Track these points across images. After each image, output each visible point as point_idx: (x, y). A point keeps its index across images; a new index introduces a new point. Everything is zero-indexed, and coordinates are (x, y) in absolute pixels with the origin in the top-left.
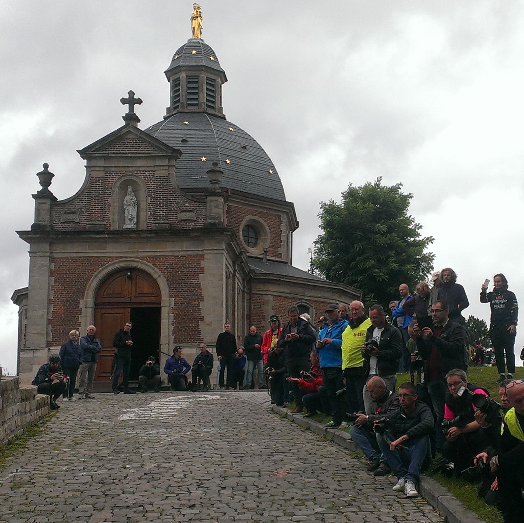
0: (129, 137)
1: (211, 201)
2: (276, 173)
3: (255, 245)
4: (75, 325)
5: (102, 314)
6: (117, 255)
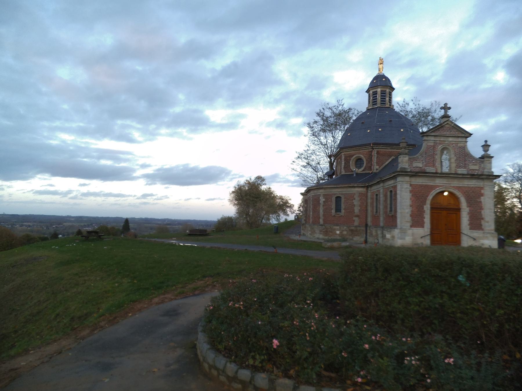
0: (447, 126)
1: (487, 160)
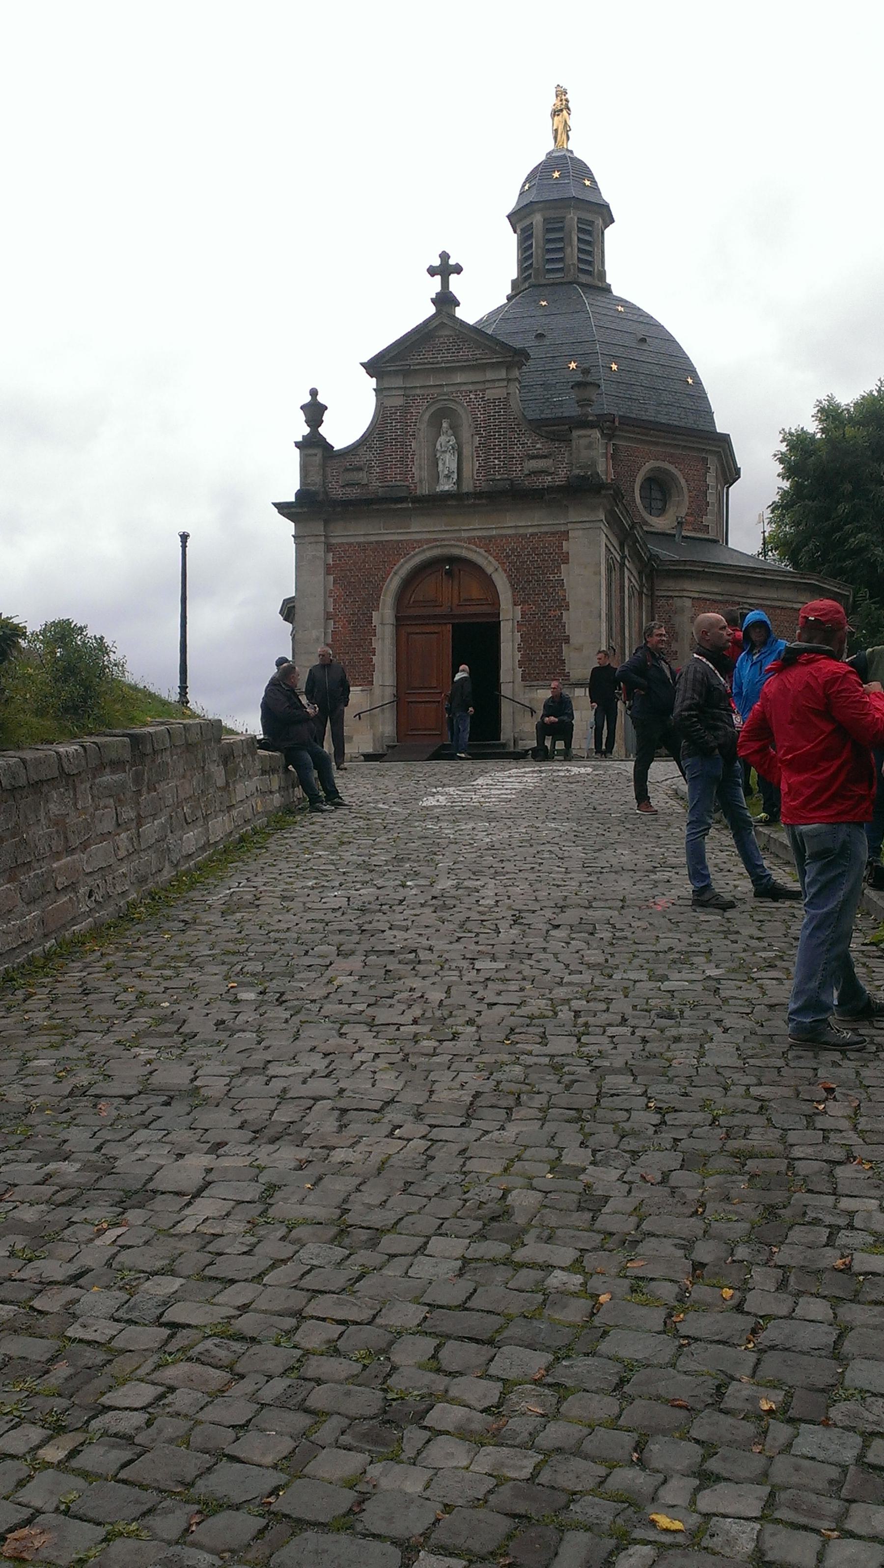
2: (698, 383)
3: (662, 511)
5: (409, 634)
6: (429, 536)
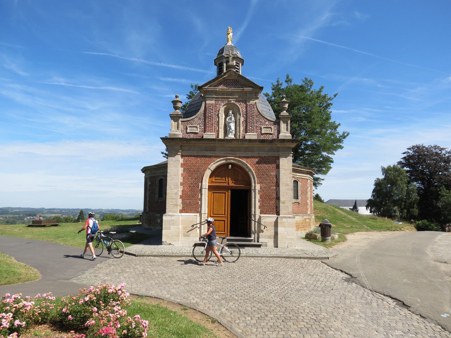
4: (197, 199)
